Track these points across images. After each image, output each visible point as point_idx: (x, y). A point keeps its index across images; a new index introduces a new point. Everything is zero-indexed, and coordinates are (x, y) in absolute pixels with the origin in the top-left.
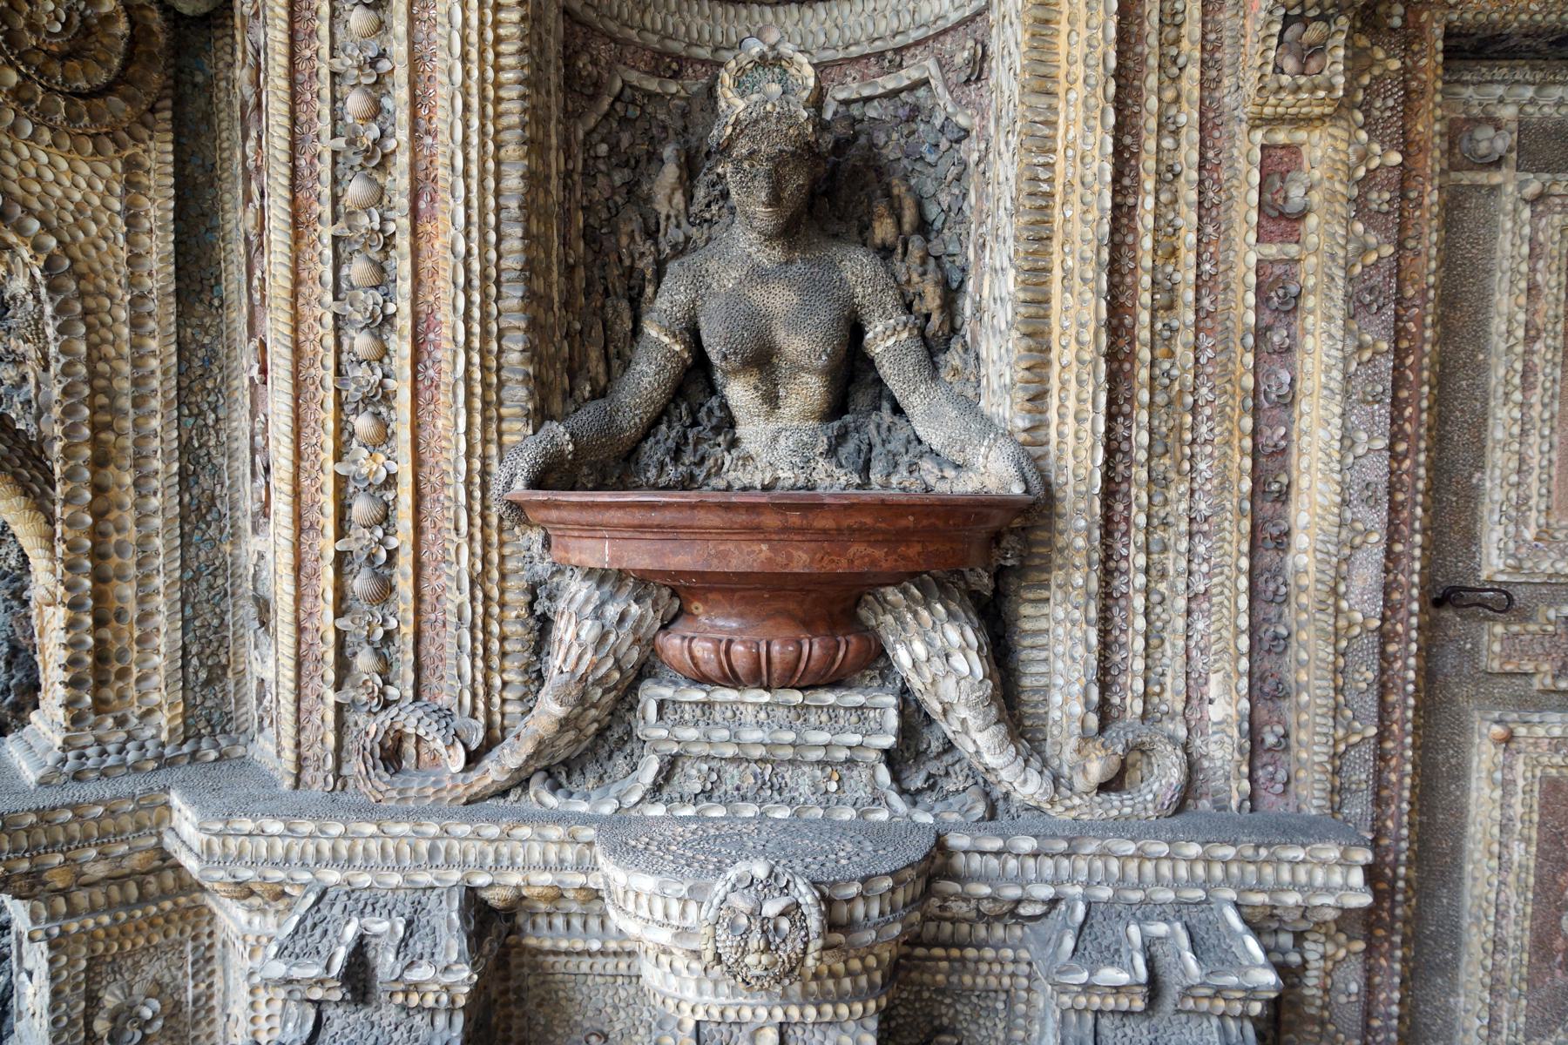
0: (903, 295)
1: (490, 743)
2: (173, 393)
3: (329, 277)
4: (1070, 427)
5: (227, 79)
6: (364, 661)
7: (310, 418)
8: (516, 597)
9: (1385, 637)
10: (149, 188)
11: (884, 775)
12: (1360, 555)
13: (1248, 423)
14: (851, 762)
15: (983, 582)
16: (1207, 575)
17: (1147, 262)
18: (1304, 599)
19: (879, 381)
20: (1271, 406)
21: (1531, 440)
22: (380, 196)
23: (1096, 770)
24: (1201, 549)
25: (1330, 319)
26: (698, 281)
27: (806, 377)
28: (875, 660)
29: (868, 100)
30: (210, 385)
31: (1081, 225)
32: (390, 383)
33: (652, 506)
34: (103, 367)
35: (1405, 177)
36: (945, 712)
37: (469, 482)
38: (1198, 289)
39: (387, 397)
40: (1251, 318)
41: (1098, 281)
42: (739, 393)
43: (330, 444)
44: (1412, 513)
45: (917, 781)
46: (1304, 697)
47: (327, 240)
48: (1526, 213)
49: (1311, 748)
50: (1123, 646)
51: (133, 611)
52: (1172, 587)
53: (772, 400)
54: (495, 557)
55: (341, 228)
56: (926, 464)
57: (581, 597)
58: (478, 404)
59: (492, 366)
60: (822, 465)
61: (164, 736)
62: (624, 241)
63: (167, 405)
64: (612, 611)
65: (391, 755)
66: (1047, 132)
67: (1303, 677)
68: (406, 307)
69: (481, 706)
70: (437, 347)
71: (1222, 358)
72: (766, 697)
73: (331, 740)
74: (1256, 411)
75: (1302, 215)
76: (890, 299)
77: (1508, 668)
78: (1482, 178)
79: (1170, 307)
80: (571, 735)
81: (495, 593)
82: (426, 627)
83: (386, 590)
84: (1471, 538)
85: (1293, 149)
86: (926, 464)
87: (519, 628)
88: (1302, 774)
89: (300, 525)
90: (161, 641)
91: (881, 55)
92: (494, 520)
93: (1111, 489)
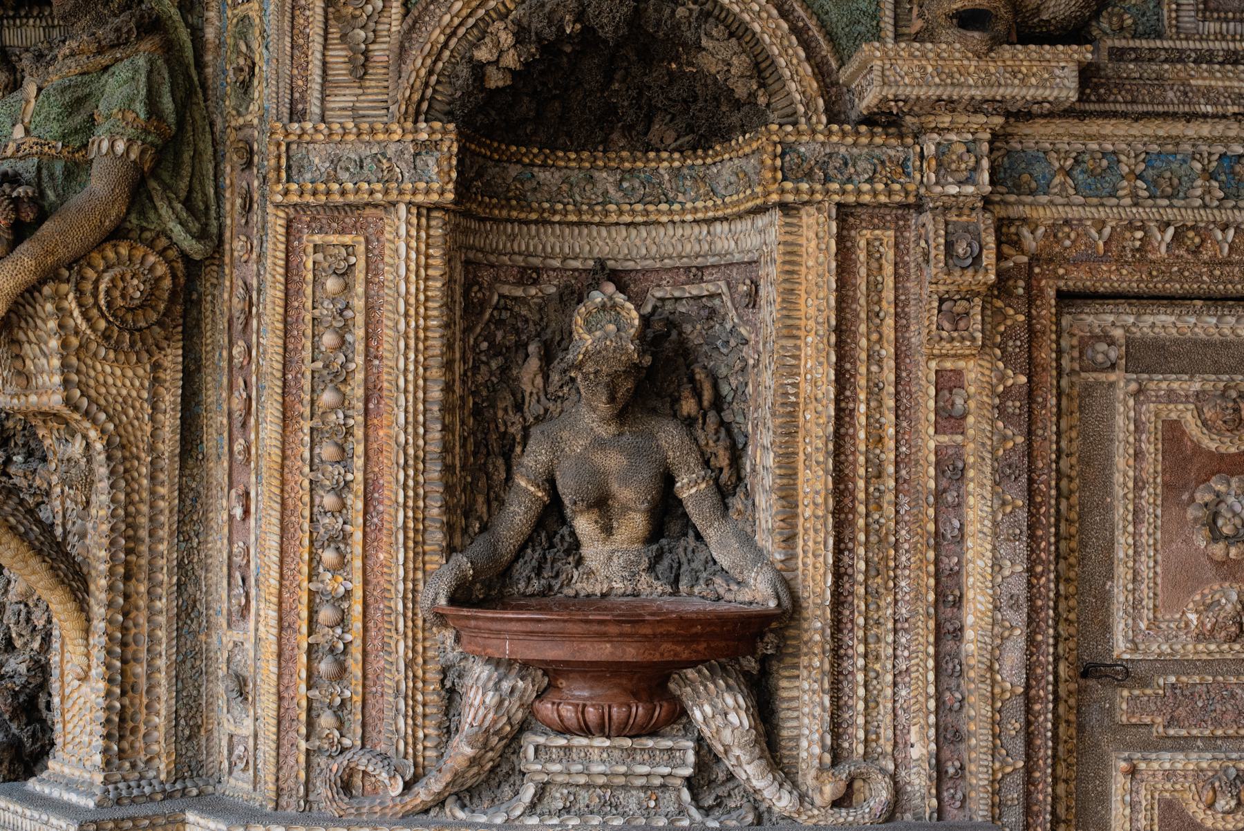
0: (702, 454)
1: (416, 779)
2: (175, 526)
3: (307, 455)
4: (810, 561)
5: (214, 296)
6: (326, 720)
7: (291, 550)
8: (433, 676)
9: (1028, 700)
10: (165, 381)
11: (686, 795)
12: (1009, 644)
13: (931, 555)
14: (663, 786)
15: (751, 664)
16: (909, 658)
17: (862, 448)
18: (972, 674)
19: (685, 515)
20: (945, 542)
21: (1143, 558)
22: (343, 403)
23: (829, 791)
24: (903, 640)
25: (982, 486)
26: (555, 445)
27: (633, 515)
28: (679, 715)
29: (677, 299)
30: (195, 518)
31: (816, 423)
32: (348, 528)
33: (539, 621)
34: (132, 509)
35: (1031, 393)
36: (726, 752)
37: (405, 598)
38: (897, 464)
39: (346, 537)
40: (932, 484)
41: (826, 463)
42: (584, 525)
43: (305, 569)
44: (1047, 614)
45: (709, 801)
46: (973, 741)
47: (307, 430)
48: (1131, 402)
49: (978, 778)
50: (850, 708)
51: (143, 685)
52: (884, 667)
53: (608, 530)
54: (420, 648)
55: (317, 422)
56: (718, 580)
57: (484, 675)
58: (411, 544)
59: (421, 518)
60: (644, 578)
61: (163, 776)
62: (500, 413)
63: (171, 535)
64: (506, 685)
65: (346, 787)
66: (793, 362)
67: (973, 727)
68: (360, 476)
69: (410, 751)
70: (381, 503)
71: (915, 511)
72: (607, 743)
73: (303, 775)
74: (937, 547)
75: (964, 417)
76: (692, 460)
77: (1133, 720)
78: (1102, 377)
79: (879, 476)
80: (475, 770)
81: (420, 673)
82: (369, 696)
83: (341, 672)
84: (1106, 628)
85: (958, 373)
86: (718, 580)
87: (435, 697)
89: (282, 626)
90: (162, 708)
91: (688, 269)
92: (420, 623)
93: (839, 600)
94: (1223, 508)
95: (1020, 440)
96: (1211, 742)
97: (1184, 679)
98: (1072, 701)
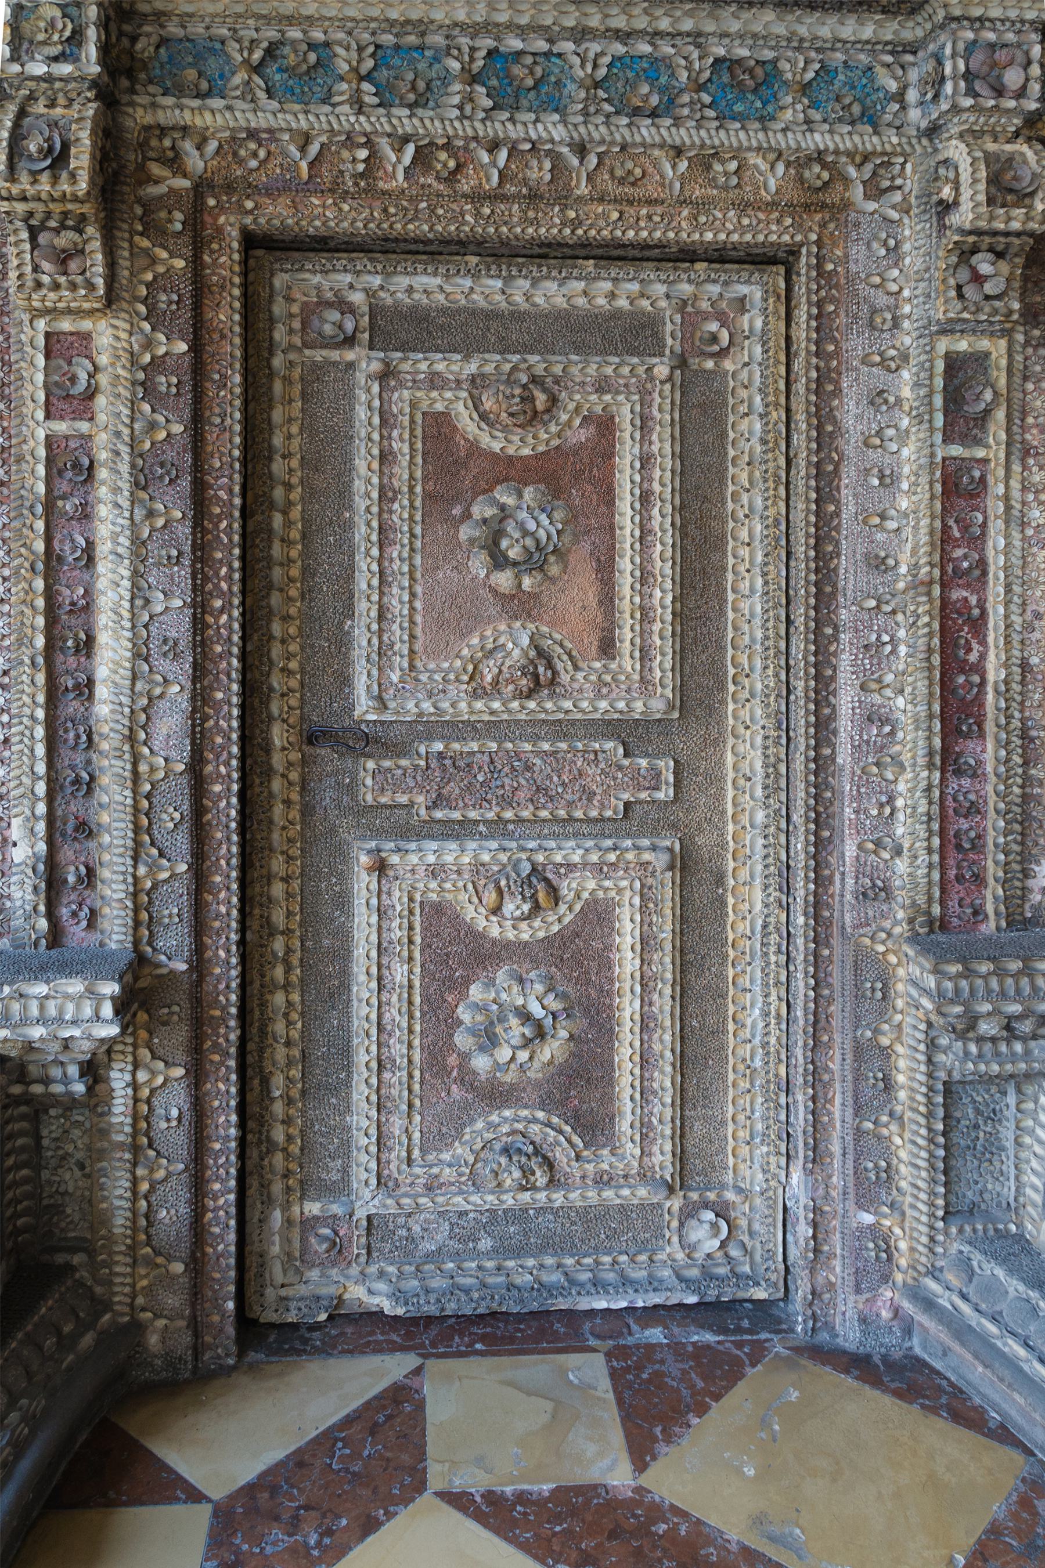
71: (16, 524)
77: (383, 800)
88: (106, 910)
94: (510, 527)
95: (177, 428)
96: (498, 828)
97: (456, 746)
98: (294, 776)
